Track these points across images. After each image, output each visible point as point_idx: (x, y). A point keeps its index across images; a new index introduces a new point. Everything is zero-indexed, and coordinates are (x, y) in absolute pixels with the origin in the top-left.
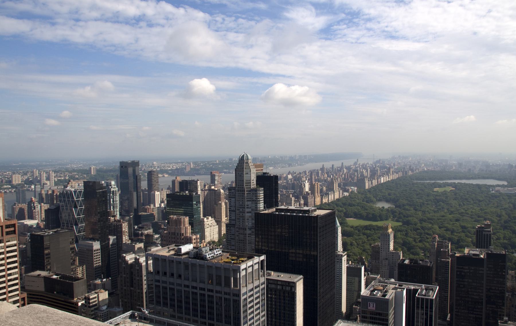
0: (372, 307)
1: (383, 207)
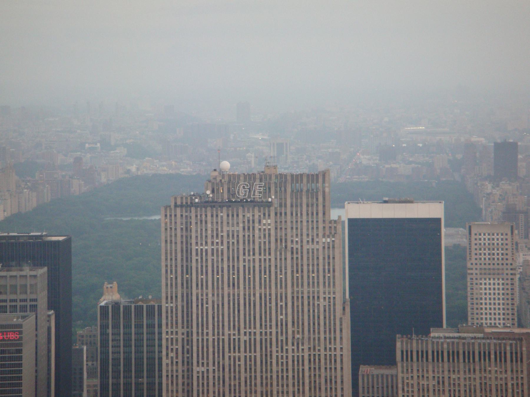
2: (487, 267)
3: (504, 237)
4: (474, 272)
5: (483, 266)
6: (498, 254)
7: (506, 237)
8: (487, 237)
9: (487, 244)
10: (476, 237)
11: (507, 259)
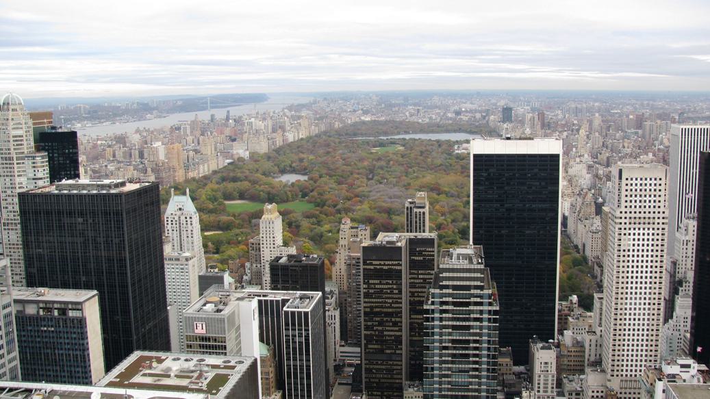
0: (200, 330)
2: (638, 215)
3: (658, 182)
4: (623, 221)
5: (633, 215)
6: (650, 201)
7: (660, 182)
8: (639, 182)
10: (627, 182)
11: (659, 207)
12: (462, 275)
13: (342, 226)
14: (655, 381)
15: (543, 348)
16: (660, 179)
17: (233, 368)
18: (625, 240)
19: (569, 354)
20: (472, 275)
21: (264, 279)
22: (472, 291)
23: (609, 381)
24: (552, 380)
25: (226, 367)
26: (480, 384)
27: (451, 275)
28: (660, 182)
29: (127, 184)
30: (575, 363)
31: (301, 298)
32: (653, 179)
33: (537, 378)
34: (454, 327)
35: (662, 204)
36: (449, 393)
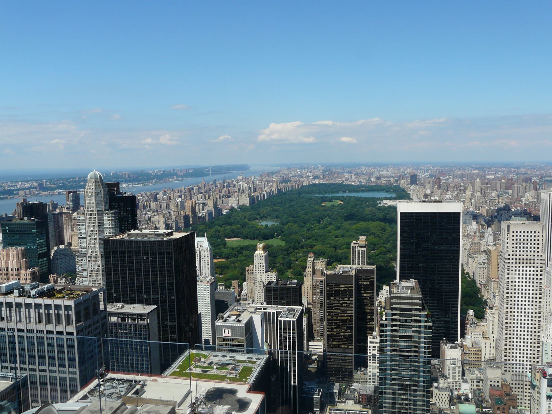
1: (267, 226)
4: (511, 261)
5: (518, 257)
7: (538, 234)
8: (522, 234)
9: (522, 240)
10: (513, 234)
11: (538, 252)
12: (406, 301)
13: (309, 259)
14: (540, 378)
15: (451, 347)
16: (539, 232)
17: (255, 362)
18: (512, 274)
19: (470, 352)
20: (414, 301)
21: (256, 293)
22: (414, 313)
23: (504, 374)
24: (458, 370)
25: (250, 362)
26: (419, 377)
27: (399, 301)
28: (538, 234)
29: (174, 233)
30: (475, 359)
31: (289, 311)
32: (533, 232)
33: (448, 368)
34: (401, 337)
35: (540, 250)
36: (397, 382)
